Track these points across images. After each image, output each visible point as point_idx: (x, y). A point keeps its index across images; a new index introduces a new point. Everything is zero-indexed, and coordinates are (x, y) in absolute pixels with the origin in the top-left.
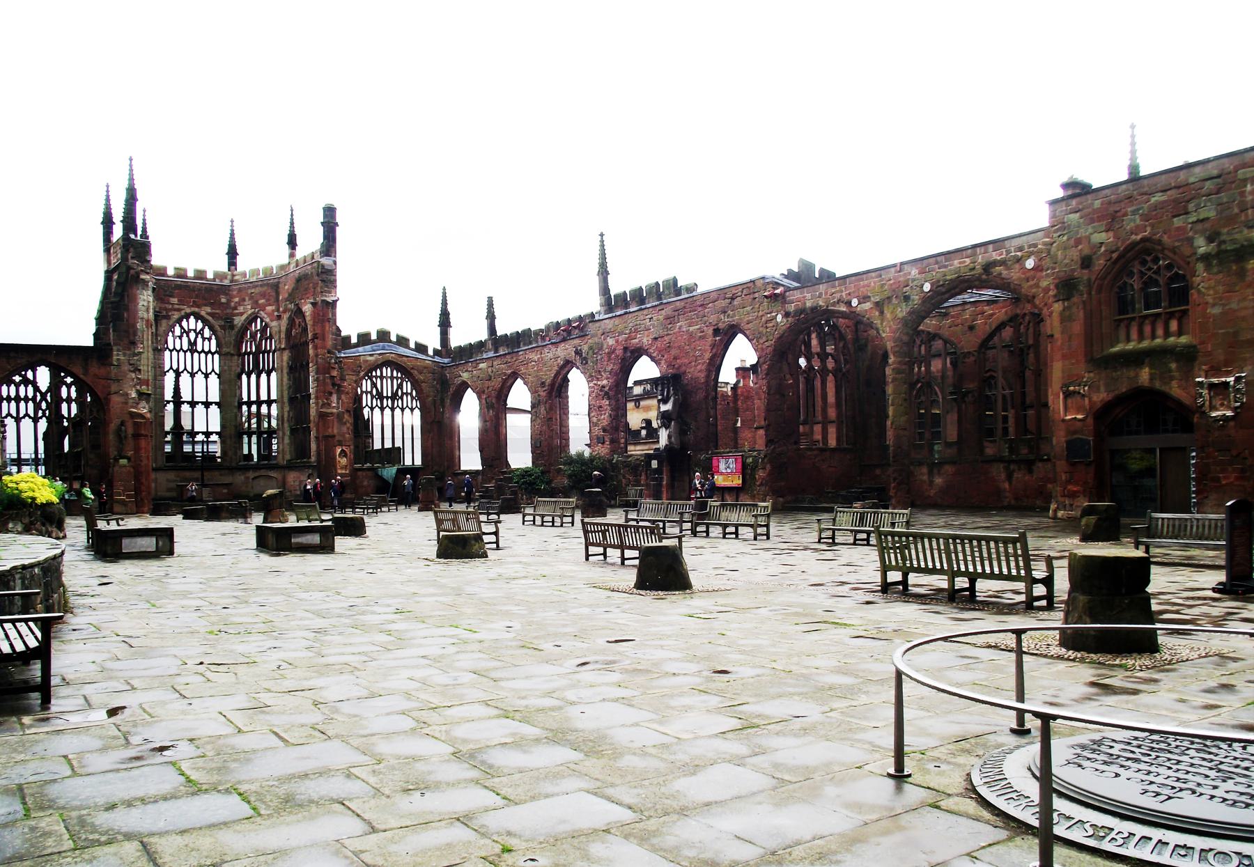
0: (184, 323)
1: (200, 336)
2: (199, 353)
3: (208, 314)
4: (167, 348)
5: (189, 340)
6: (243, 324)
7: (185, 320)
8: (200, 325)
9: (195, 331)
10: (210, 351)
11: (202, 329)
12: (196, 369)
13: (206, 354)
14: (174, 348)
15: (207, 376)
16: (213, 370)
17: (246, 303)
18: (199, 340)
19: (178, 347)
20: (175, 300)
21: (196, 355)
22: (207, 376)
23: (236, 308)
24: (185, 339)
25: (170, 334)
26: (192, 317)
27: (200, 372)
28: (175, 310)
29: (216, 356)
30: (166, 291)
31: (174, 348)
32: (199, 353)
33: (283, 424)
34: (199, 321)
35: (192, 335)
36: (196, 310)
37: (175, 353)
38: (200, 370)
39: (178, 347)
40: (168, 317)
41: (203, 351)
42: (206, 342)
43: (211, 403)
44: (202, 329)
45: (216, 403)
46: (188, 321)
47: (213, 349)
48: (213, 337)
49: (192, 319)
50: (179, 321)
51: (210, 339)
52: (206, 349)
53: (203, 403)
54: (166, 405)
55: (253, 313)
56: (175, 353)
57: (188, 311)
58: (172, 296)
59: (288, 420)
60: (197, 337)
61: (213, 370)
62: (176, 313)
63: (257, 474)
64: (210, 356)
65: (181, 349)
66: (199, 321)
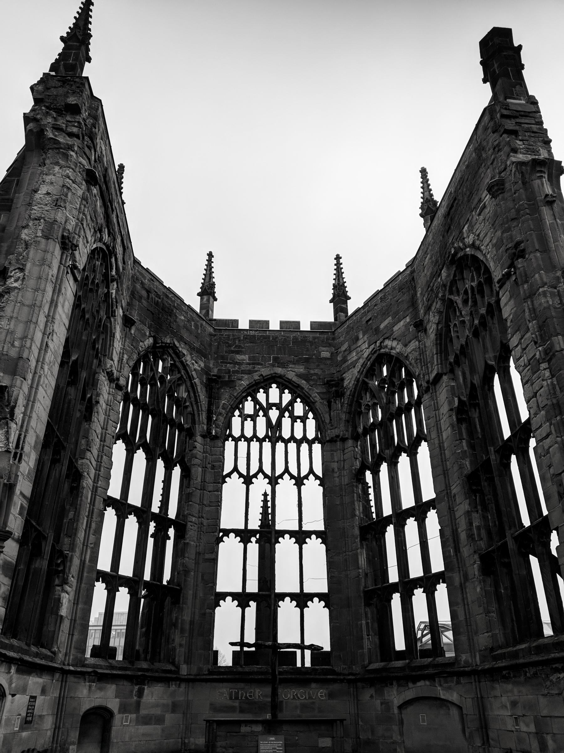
0: (261, 396)
1: (287, 414)
2: (286, 442)
3: (299, 376)
4: (231, 435)
5: (269, 421)
6: (357, 380)
7: (262, 391)
8: (287, 397)
9: (278, 406)
10: (304, 439)
11: (291, 403)
12: (280, 469)
13: (299, 443)
14: (243, 436)
15: (299, 481)
16: (311, 471)
17: (360, 342)
18: (286, 422)
19: (249, 433)
20: (244, 358)
21: (280, 446)
22: (299, 481)
23: (345, 360)
24: (261, 421)
25: (237, 413)
26: (274, 386)
27: (286, 476)
28: (243, 372)
29: (317, 448)
30: (230, 346)
31: (243, 436)
32: (286, 442)
33: (457, 550)
34: (286, 391)
35: (274, 414)
36: (279, 370)
37: (243, 445)
38: (287, 470)
39: (249, 433)
40: (230, 384)
41: (292, 438)
42: (299, 425)
43: (309, 534)
44: (291, 403)
45: (318, 534)
46: (267, 392)
47: (311, 435)
48: (311, 415)
49: (274, 391)
50: (252, 392)
51: (304, 419)
52: (299, 435)
53: (292, 534)
54: (221, 540)
55: (372, 353)
56: (243, 445)
57: (266, 371)
58: (238, 352)
59: (470, 536)
60: (281, 416)
61: (311, 471)
62: (246, 376)
63: (409, 694)
64: (305, 447)
65: (255, 435)
66: (286, 391)
